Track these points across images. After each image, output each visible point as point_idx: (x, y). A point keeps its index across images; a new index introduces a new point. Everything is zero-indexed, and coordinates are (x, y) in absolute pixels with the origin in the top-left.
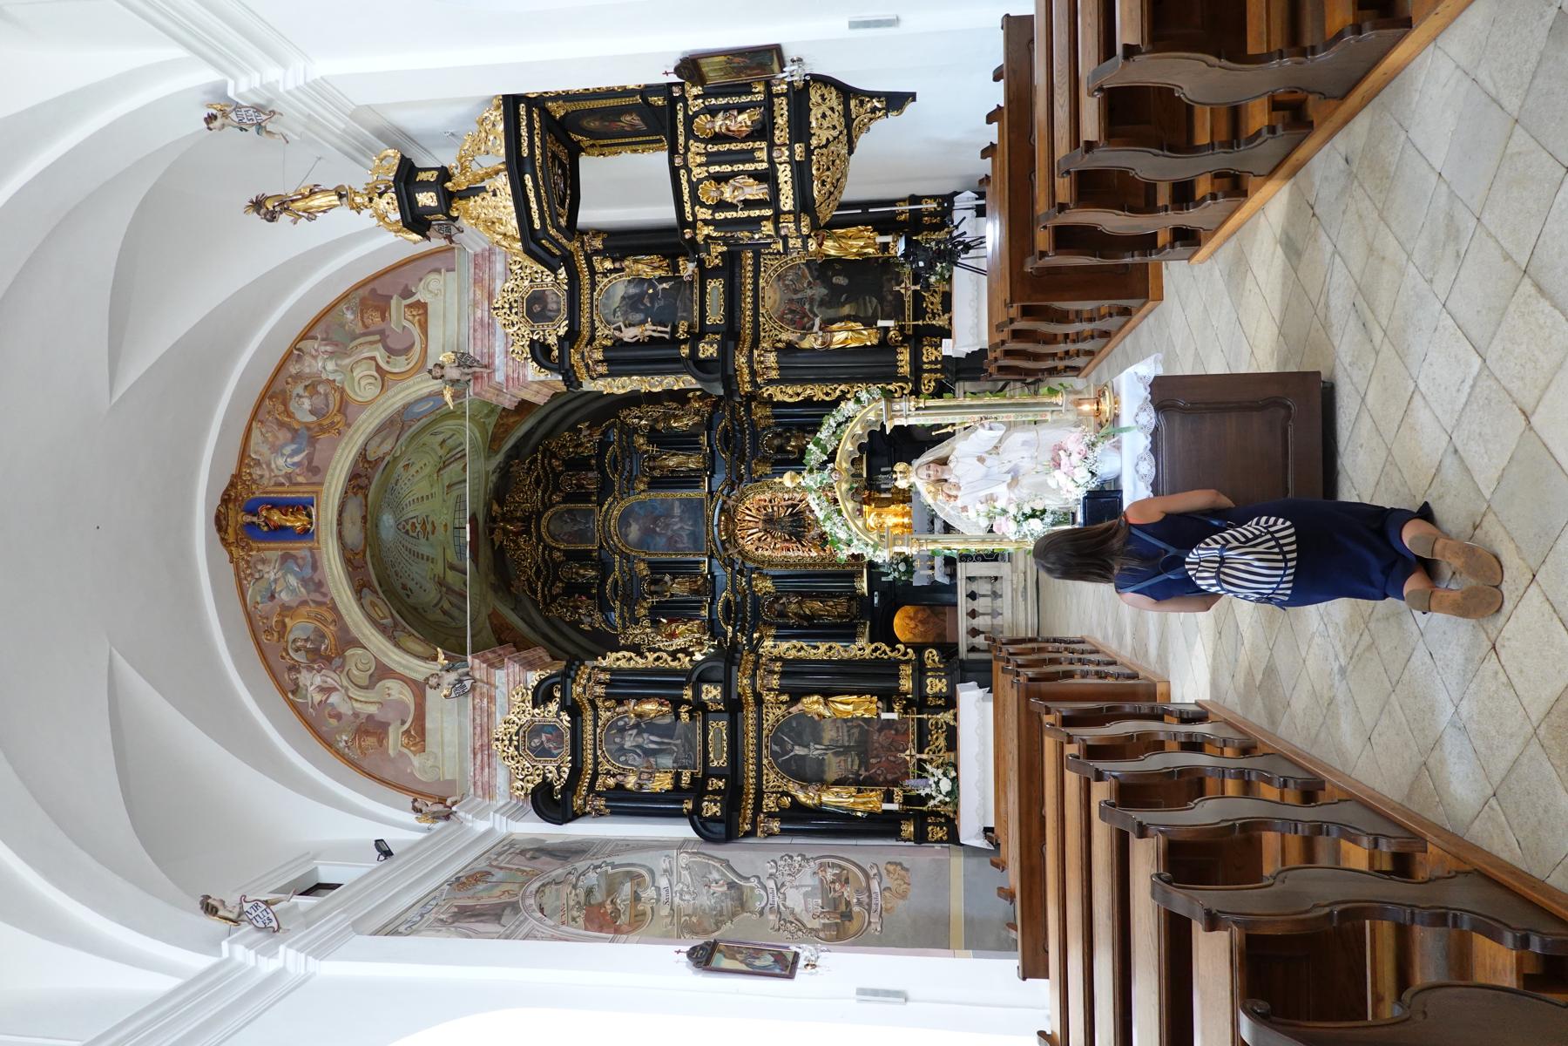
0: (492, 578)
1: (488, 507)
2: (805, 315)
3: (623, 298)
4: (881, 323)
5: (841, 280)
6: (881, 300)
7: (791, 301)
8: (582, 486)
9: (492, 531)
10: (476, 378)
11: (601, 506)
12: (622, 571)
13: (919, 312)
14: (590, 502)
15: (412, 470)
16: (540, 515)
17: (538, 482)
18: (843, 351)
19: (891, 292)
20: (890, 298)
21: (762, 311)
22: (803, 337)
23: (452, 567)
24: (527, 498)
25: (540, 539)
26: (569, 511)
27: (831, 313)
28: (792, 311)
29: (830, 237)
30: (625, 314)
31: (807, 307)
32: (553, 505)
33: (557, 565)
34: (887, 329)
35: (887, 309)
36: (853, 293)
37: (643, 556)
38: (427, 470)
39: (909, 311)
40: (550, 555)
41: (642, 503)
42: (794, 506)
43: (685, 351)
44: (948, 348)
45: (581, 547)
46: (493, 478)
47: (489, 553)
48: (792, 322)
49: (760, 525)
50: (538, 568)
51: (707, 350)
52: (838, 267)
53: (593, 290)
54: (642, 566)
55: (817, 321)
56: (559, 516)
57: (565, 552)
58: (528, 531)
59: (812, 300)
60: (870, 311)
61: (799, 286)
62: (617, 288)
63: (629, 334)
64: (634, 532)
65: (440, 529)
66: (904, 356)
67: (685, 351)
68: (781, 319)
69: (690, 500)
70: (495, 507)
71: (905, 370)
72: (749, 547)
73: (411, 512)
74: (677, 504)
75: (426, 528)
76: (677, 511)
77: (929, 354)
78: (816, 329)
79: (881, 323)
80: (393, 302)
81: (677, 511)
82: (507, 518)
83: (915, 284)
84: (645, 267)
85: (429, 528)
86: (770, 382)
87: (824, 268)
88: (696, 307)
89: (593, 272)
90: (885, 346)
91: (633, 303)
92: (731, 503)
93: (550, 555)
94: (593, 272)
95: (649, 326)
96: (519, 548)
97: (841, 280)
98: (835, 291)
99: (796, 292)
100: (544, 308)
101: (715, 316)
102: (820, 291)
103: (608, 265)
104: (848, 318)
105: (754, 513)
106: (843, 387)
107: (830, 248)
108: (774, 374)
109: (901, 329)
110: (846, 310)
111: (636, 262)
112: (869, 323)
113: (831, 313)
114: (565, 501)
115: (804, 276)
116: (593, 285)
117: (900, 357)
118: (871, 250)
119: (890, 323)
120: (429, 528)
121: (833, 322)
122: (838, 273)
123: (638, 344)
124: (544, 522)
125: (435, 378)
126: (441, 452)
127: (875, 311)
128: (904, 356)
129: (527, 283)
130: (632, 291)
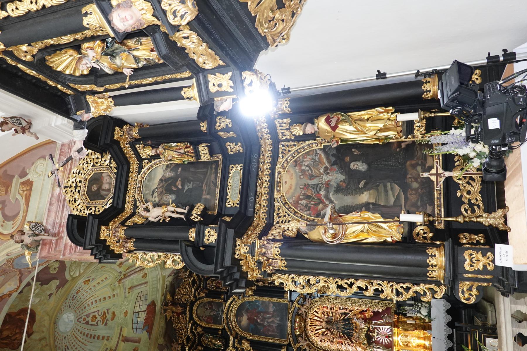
0: (161, 341)
1: (164, 295)
2: (320, 201)
3: (161, 180)
4: (405, 217)
5: (359, 166)
6: (405, 188)
7: (306, 186)
8: (219, 288)
9: (165, 311)
10: (44, 244)
11: (226, 302)
12: (234, 346)
13: (452, 203)
14: (220, 298)
15: (92, 284)
16: (192, 303)
17: (194, 282)
18: (358, 246)
19: (417, 178)
20: (415, 185)
21: (276, 195)
22: (312, 225)
23: (126, 340)
24: (188, 293)
25: (191, 318)
26: (210, 303)
27: (349, 200)
28: (308, 197)
29: (345, 121)
30: (161, 194)
31: (323, 193)
32: (200, 298)
33: (200, 336)
34: (412, 225)
35: (413, 198)
36: (370, 180)
37: (249, 337)
38: (108, 281)
39: (439, 201)
40: (196, 329)
41: (250, 302)
42: (346, 314)
43: (192, 235)
44: (505, 256)
45: (215, 326)
46: (170, 279)
47: (163, 324)
48: (307, 208)
49: (323, 324)
50: (188, 337)
51: (211, 236)
52: (356, 152)
53: (139, 172)
54: (246, 345)
55: (329, 211)
56: (204, 305)
57: (204, 328)
58: (184, 313)
59: (328, 186)
60: (392, 200)
61: (315, 172)
62: (159, 172)
63: (155, 214)
64: (245, 321)
65: (120, 316)
66: (437, 260)
67: (192, 235)
68: (296, 204)
69: (280, 304)
70: (169, 296)
71: (437, 273)
72: (316, 339)
73: (92, 309)
74: (271, 305)
75: (106, 317)
76: (271, 310)
77: (473, 261)
78: (327, 219)
79: (405, 217)
80: (14, 180)
81: (271, 310)
82: (174, 303)
83: (446, 169)
84: (175, 153)
85: (109, 317)
86: (279, 271)
87: (343, 153)
88: (218, 191)
89: (140, 159)
90: (409, 242)
91: (167, 185)
92: (303, 310)
93: (196, 329)
94: (140, 159)
95: (171, 208)
96: (180, 323)
97: (359, 166)
98: (353, 177)
99: (312, 177)
100: (100, 188)
101: (233, 199)
102: (337, 177)
103: (149, 152)
104: (367, 207)
105: (319, 315)
106: (361, 283)
107: (347, 131)
108: (281, 264)
109: (430, 225)
110: (365, 197)
111: (169, 148)
112: (390, 214)
113: (349, 200)
114: (207, 296)
115: (320, 162)
116: (141, 168)
117: (432, 261)
118: (391, 134)
119: (418, 218)
120: (109, 317)
121: (348, 210)
122: (355, 159)
123: (160, 224)
124: (195, 308)
125: (17, 242)
126: (121, 270)
127: (398, 199)
128: (437, 260)
129: (90, 167)
130: (169, 174)
